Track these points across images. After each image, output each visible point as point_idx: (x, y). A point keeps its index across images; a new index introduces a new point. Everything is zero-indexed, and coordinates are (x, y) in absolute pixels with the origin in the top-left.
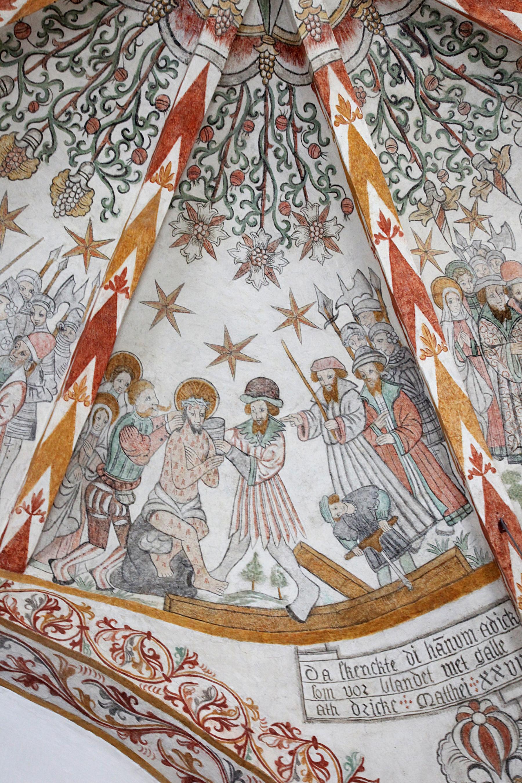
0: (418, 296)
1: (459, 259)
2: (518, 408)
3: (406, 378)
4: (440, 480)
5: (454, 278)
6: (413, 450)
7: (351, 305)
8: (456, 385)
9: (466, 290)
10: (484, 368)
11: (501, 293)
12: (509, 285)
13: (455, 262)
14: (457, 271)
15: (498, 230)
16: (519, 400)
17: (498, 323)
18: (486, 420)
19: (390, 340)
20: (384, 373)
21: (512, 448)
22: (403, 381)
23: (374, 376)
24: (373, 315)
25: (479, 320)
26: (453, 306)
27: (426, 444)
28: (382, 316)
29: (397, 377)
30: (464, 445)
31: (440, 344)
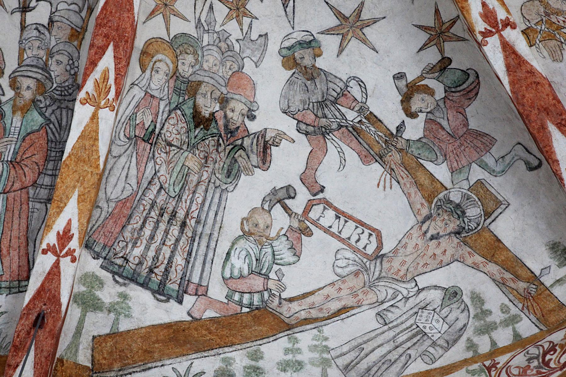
0: (121, 37)
1: (196, 35)
2: (151, 219)
3: (59, 117)
4: (17, 240)
5: (178, 51)
6: (13, 194)
7: (54, 6)
8: (97, 151)
9: (181, 71)
10: (145, 159)
11: (215, 99)
12: (228, 96)
13: (189, 36)
14: (186, 46)
15: (254, 36)
16: (157, 212)
17: (192, 125)
18: (110, 210)
19: (68, 68)
20: (41, 98)
21: (115, 254)
22: (53, 118)
23: (27, 95)
24: (68, 31)
25: (175, 109)
26: (156, 77)
27: (31, 196)
28: (77, 37)
29: (50, 110)
30: (62, 215)
31: (111, 99)
